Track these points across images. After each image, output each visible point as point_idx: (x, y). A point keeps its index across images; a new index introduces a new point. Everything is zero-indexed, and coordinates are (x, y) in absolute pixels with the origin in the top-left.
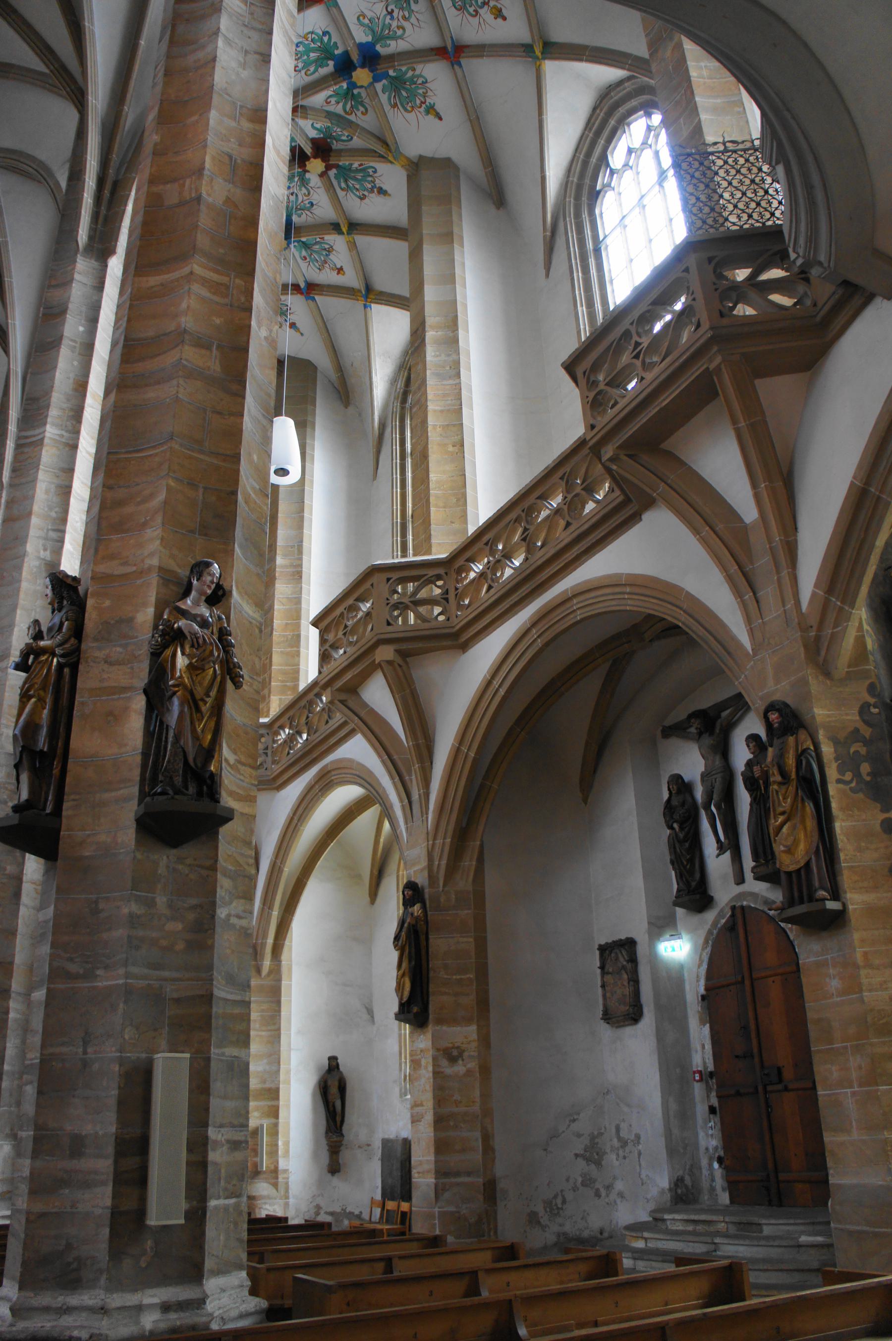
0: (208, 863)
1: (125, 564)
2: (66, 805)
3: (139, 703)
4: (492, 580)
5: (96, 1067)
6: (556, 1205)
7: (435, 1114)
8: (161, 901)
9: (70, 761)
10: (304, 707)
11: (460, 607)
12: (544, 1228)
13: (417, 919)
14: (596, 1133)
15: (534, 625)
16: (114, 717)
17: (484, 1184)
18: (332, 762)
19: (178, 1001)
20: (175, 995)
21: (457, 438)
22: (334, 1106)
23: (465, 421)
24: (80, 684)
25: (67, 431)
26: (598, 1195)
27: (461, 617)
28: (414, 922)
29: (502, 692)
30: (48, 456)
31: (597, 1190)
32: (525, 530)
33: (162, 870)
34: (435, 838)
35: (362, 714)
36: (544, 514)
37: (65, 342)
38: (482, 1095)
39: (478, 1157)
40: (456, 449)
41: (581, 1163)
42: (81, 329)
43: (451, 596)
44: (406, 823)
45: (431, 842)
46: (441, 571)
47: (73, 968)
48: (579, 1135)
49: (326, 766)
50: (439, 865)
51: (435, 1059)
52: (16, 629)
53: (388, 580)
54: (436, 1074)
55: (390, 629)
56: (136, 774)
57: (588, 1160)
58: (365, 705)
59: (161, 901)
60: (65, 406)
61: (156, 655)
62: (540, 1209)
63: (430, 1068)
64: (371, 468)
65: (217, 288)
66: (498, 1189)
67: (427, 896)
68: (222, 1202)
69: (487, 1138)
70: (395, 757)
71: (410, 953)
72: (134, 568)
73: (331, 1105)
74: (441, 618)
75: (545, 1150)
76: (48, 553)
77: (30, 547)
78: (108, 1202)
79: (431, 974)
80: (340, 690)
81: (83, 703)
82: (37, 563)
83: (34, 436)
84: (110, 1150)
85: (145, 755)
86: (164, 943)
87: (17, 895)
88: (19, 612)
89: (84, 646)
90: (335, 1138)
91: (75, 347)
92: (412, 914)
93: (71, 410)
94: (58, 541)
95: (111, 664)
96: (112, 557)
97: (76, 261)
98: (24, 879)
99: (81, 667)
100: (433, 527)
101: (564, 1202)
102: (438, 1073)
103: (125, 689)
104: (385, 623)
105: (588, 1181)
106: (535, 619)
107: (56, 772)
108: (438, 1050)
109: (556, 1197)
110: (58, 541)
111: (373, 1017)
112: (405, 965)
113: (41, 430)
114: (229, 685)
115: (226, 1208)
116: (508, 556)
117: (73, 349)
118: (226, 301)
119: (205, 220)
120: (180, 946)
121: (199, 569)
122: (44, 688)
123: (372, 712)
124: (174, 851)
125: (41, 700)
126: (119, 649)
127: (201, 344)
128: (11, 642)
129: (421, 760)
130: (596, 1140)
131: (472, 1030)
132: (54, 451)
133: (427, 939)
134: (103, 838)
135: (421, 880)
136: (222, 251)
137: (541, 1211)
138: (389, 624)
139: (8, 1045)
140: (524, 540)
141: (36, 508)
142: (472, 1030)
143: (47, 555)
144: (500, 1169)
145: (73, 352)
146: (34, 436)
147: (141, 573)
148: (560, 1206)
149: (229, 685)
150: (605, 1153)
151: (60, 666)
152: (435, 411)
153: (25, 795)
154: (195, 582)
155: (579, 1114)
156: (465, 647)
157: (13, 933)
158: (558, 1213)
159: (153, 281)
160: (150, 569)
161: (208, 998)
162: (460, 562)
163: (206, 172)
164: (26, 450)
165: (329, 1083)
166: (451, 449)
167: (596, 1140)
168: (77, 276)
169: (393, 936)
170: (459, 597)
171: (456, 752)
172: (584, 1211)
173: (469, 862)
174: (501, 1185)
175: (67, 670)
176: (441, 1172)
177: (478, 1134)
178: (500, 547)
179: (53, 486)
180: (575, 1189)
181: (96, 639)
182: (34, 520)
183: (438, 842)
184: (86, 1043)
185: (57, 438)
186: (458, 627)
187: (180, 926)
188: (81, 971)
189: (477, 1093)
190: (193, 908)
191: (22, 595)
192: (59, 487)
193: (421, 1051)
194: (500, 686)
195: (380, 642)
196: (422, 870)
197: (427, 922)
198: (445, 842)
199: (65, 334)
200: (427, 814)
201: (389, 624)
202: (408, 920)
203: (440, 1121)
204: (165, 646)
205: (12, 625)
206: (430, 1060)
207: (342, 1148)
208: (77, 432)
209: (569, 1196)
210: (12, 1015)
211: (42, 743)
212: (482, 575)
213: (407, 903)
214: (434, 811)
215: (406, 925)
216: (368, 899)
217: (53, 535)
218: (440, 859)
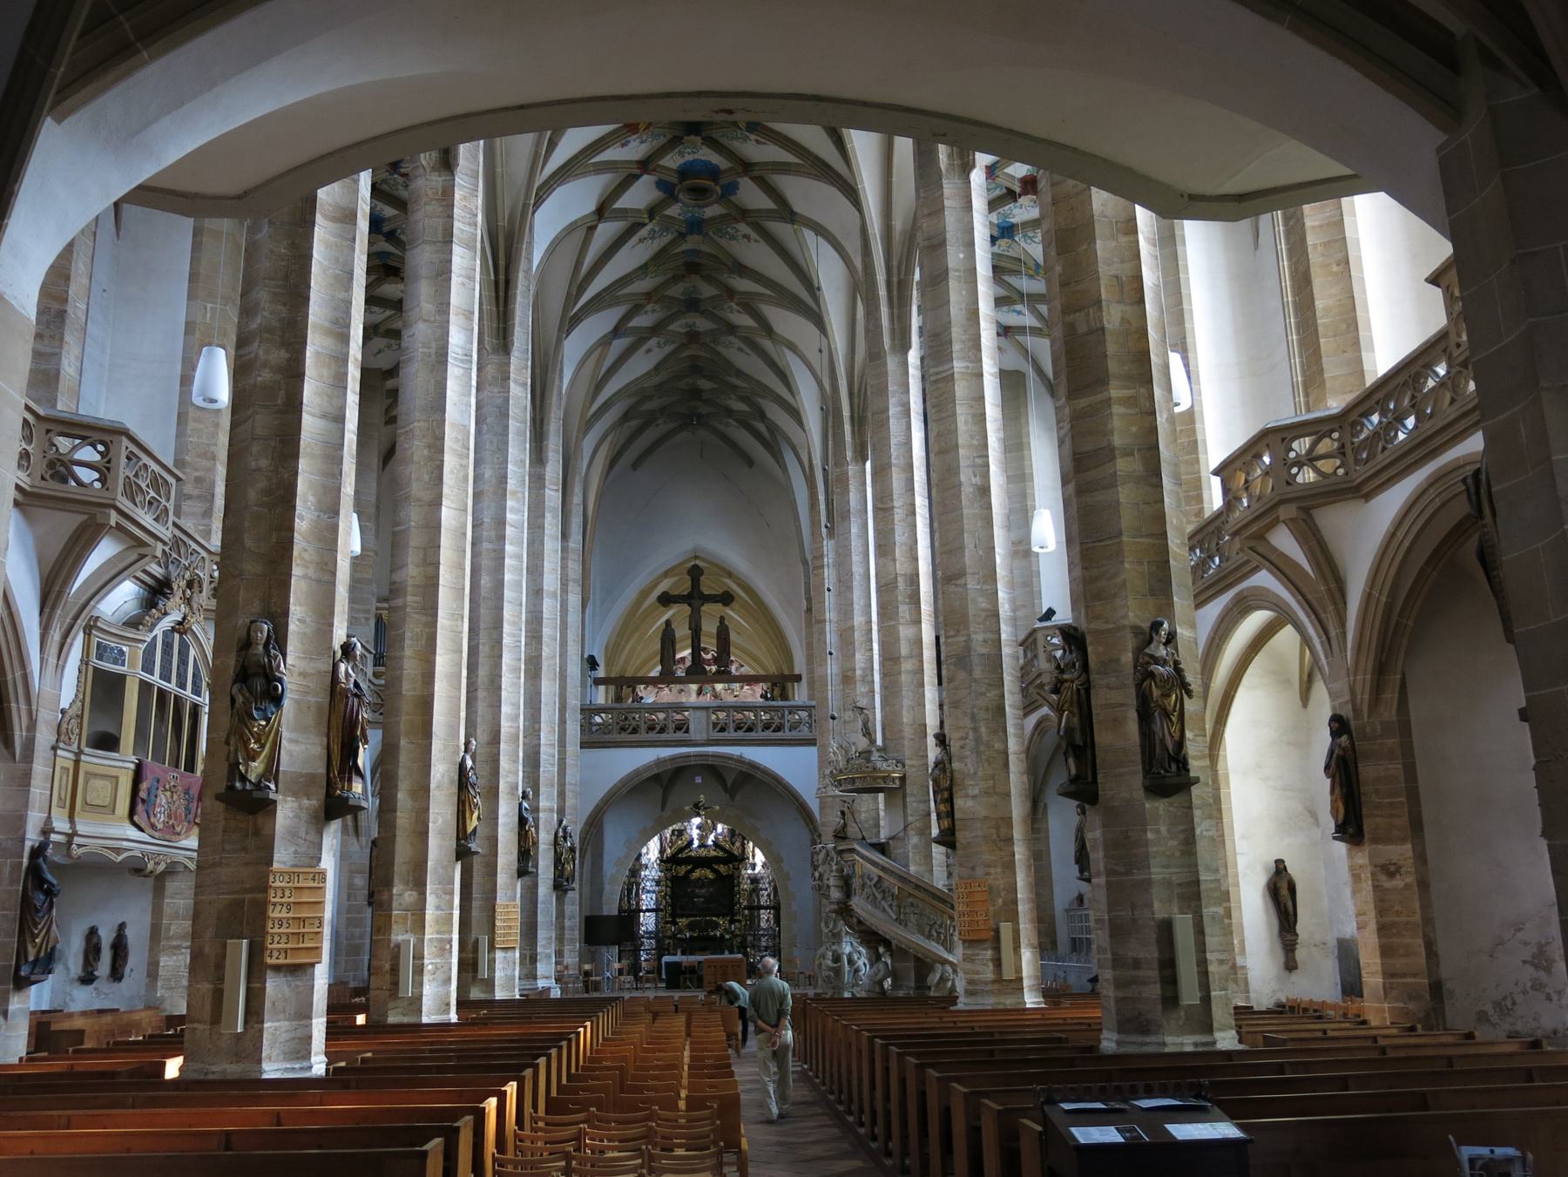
0: (1187, 804)
1: (1107, 622)
2: (1099, 777)
3: (1133, 715)
4: (1386, 441)
5: (1140, 922)
6: (1506, 1006)
7: (1378, 922)
8: (1163, 829)
9: (1097, 750)
10: (1213, 532)
11: (1357, 462)
12: (1494, 1025)
13: (1344, 749)
14: (1543, 942)
15: (1431, 485)
16: (1118, 723)
17: (1430, 985)
18: (1248, 589)
19: (1180, 885)
20: (1178, 882)
21: (1340, 256)
22: (1285, 906)
23: (1348, 234)
24: (1093, 702)
25: (970, 362)
26: (1549, 998)
27: (1361, 472)
28: (1341, 753)
29: (1407, 544)
30: (961, 389)
31: (1548, 994)
32: (1413, 397)
33: (1161, 812)
34: (1355, 675)
35: (1273, 558)
36: (1431, 383)
37: (952, 274)
38: (1422, 907)
39: (1421, 960)
40: (1341, 268)
41: (1530, 969)
42: (961, 256)
43: (1348, 450)
44: (1327, 658)
45: (1352, 678)
46: (1336, 426)
47: (1117, 868)
48: (1526, 944)
49: (1242, 591)
50: (1362, 699)
51: (1373, 874)
52: (967, 550)
53: (1283, 440)
54: (1376, 887)
55: (1290, 488)
56: (1138, 758)
57: (1537, 967)
58: (1275, 549)
59: (1163, 829)
60: (964, 338)
61: (1139, 686)
62: (1489, 1008)
63: (1370, 883)
64: (1250, 238)
65: (1130, 402)
66: (1444, 989)
67: (1353, 728)
68: (1218, 993)
69: (1430, 945)
70: (1309, 597)
71: (1341, 781)
72: (1112, 626)
73: (1282, 906)
74: (1341, 472)
75: (1491, 956)
76: (978, 478)
77: (963, 478)
78: (1159, 992)
79: (1363, 799)
80: (1248, 538)
81: (1097, 714)
82: (971, 490)
83: (944, 371)
84: (1156, 965)
85: (1142, 746)
86: (1168, 853)
87: (1006, 765)
88: (966, 535)
89: (1091, 678)
90: (1289, 937)
91: (960, 276)
92: (1340, 746)
93: (970, 340)
94: (984, 466)
95: (1110, 688)
96: (1098, 618)
97: (941, 187)
98: (1009, 751)
99: (1092, 692)
100: (1324, 360)
101: (1514, 1003)
102: (1378, 886)
103: (1122, 705)
104: (1285, 484)
105: (1537, 986)
106: (1432, 481)
107: (1090, 757)
108: (1376, 866)
109: (1505, 998)
110: (984, 466)
111: (1317, 820)
112: (1337, 791)
113: (949, 366)
114: (1185, 696)
115: (1220, 997)
116: (1400, 419)
117: (959, 279)
118: (1137, 410)
119: (1111, 348)
120: (1177, 854)
121: (1156, 626)
122: (1071, 704)
123: (1282, 555)
124: (1167, 800)
125: (1070, 712)
126: (1114, 679)
127: (1128, 453)
128: (964, 562)
129: (1335, 604)
130: (1545, 949)
131: (1407, 849)
132: (965, 383)
133: (1356, 767)
134: (1125, 795)
135: (1347, 712)
136: (1126, 368)
137: (1491, 1012)
138: (1288, 483)
139: (1018, 879)
140: (1413, 406)
141: (960, 441)
142: (1407, 849)
143: (977, 480)
144: (1444, 972)
145: (960, 282)
146: (944, 371)
147: (1120, 628)
148: (1510, 1007)
149: (1185, 696)
150: (1554, 961)
151: (1078, 690)
152: (1313, 227)
153: (1073, 771)
154: (1155, 636)
155: (1524, 924)
156: (1368, 497)
157: (1008, 795)
158: (1508, 1013)
159: (1083, 402)
160: (1124, 627)
161: (1197, 882)
162: (1354, 416)
163: (1104, 304)
164: (940, 385)
165: (1279, 885)
166: (1335, 268)
167: (1545, 949)
168: (947, 203)
169: (1323, 765)
170: (1357, 451)
171: (1368, 598)
172: (1536, 1013)
173: (1391, 695)
174: (1448, 985)
175: (1082, 692)
176: (1388, 974)
177: (1420, 941)
178: (1392, 406)
179: (970, 417)
180: (1524, 992)
181: (1098, 673)
182: (962, 452)
183: (1358, 677)
184: (1133, 910)
185: (964, 370)
186: (1355, 484)
187: (1175, 843)
188: (1124, 870)
189: (1417, 905)
190: (1182, 831)
191: (965, 521)
192: (974, 416)
193: (1361, 867)
194: (1404, 538)
195: (1281, 502)
196: (1347, 703)
197: (1354, 749)
198: (1365, 678)
199: (950, 266)
200: (1346, 651)
201: (1288, 483)
202: (1337, 751)
203: (1382, 929)
204: (1143, 681)
205: (962, 548)
206: (1369, 875)
207: (1297, 946)
208: (980, 360)
209: (1519, 998)
210: (1017, 857)
211: (1078, 740)
212: (1375, 435)
213: (1335, 734)
214: (1352, 649)
215: (1335, 756)
216: (1300, 703)
217: (978, 461)
218: (1362, 693)
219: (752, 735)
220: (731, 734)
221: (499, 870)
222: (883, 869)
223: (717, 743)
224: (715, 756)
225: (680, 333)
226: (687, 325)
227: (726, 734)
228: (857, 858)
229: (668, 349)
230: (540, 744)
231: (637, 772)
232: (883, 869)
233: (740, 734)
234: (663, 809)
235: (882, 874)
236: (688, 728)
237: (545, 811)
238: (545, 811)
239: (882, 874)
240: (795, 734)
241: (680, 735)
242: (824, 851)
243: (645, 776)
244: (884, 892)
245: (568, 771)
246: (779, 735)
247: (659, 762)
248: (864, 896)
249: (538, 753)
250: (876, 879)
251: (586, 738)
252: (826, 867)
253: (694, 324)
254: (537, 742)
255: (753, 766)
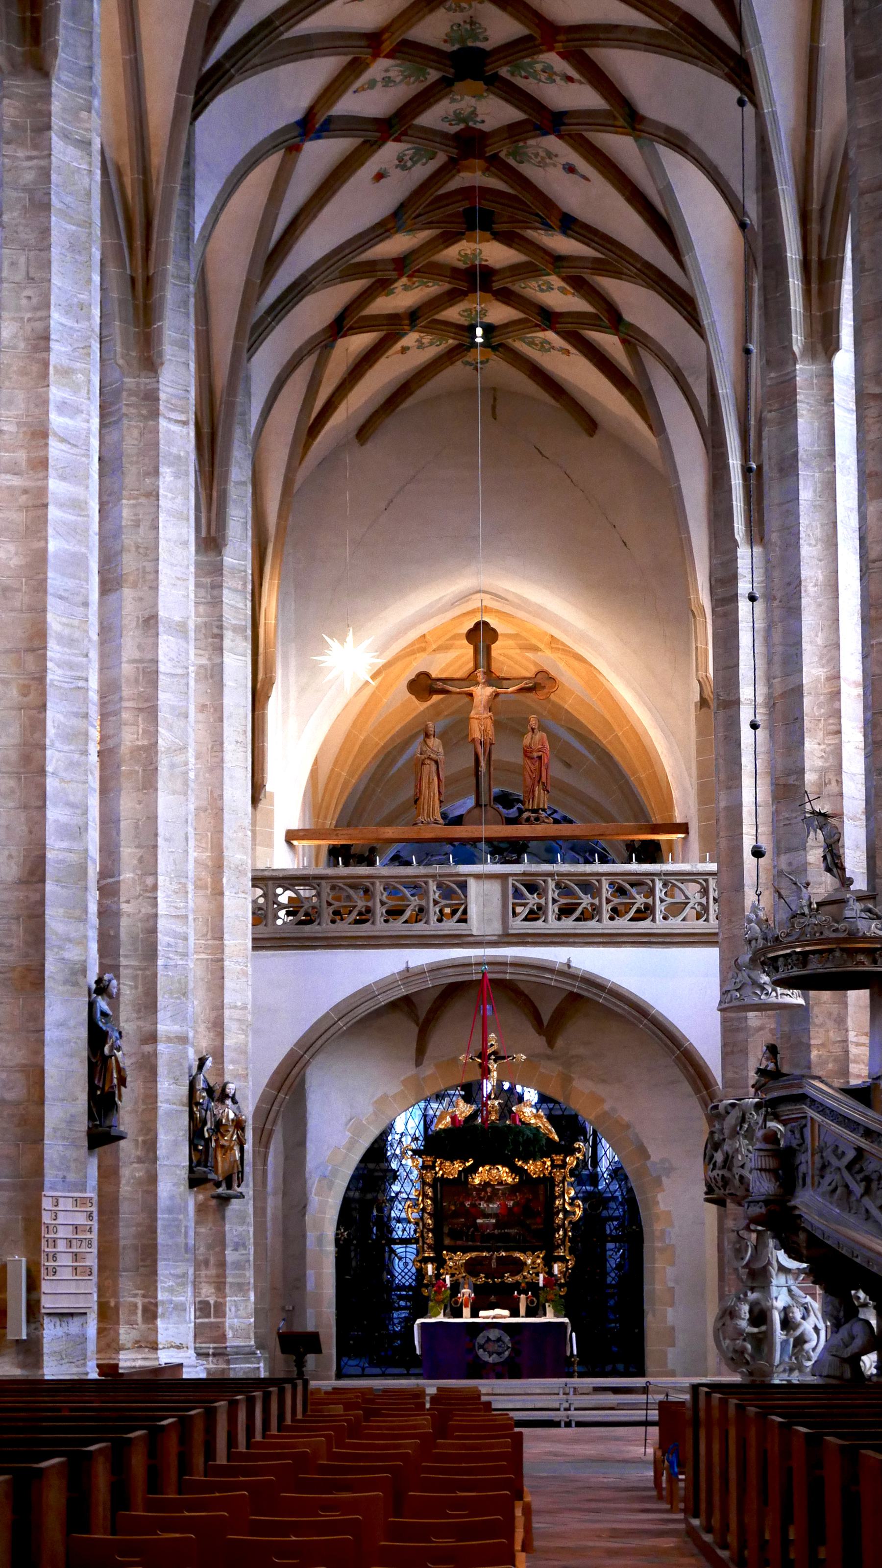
219: (591, 926)
220: (552, 924)
221: (48, 1130)
222: (868, 1133)
223: (523, 940)
224: (518, 964)
225: (445, 135)
226: (459, 117)
227: (539, 923)
228: (811, 1113)
229: (422, 171)
230: (156, 915)
231: (366, 993)
232: (868, 1133)
233: (568, 924)
234: (419, 1062)
235: (864, 1143)
236: (465, 912)
237: (169, 1040)
238: (169, 1040)
239: (864, 1143)
240: (675, 924)
241: (450, 926)
242: (735, 1114)
243: (384, 1000)
244: (868, 1180)
245: (229, 984)
246: (644, 926)
247: (408, 975)
248: (825, 1187)
249: (154, 931)
250: (851, 1155)
251: (264, 931)
252: (743, 1143)
253: (474, 113)
254: (150, 910)
255: (592, 982)
